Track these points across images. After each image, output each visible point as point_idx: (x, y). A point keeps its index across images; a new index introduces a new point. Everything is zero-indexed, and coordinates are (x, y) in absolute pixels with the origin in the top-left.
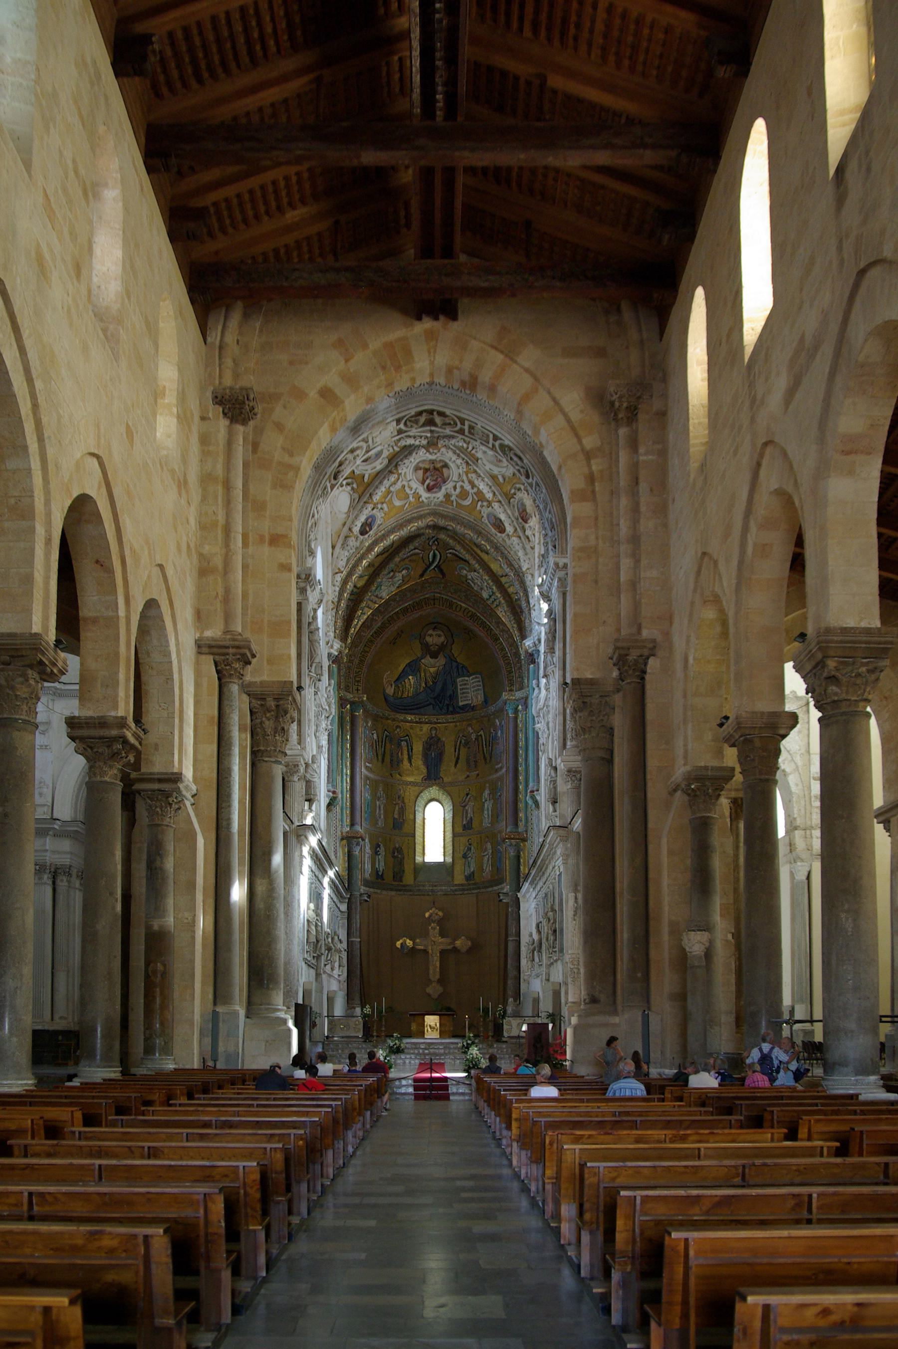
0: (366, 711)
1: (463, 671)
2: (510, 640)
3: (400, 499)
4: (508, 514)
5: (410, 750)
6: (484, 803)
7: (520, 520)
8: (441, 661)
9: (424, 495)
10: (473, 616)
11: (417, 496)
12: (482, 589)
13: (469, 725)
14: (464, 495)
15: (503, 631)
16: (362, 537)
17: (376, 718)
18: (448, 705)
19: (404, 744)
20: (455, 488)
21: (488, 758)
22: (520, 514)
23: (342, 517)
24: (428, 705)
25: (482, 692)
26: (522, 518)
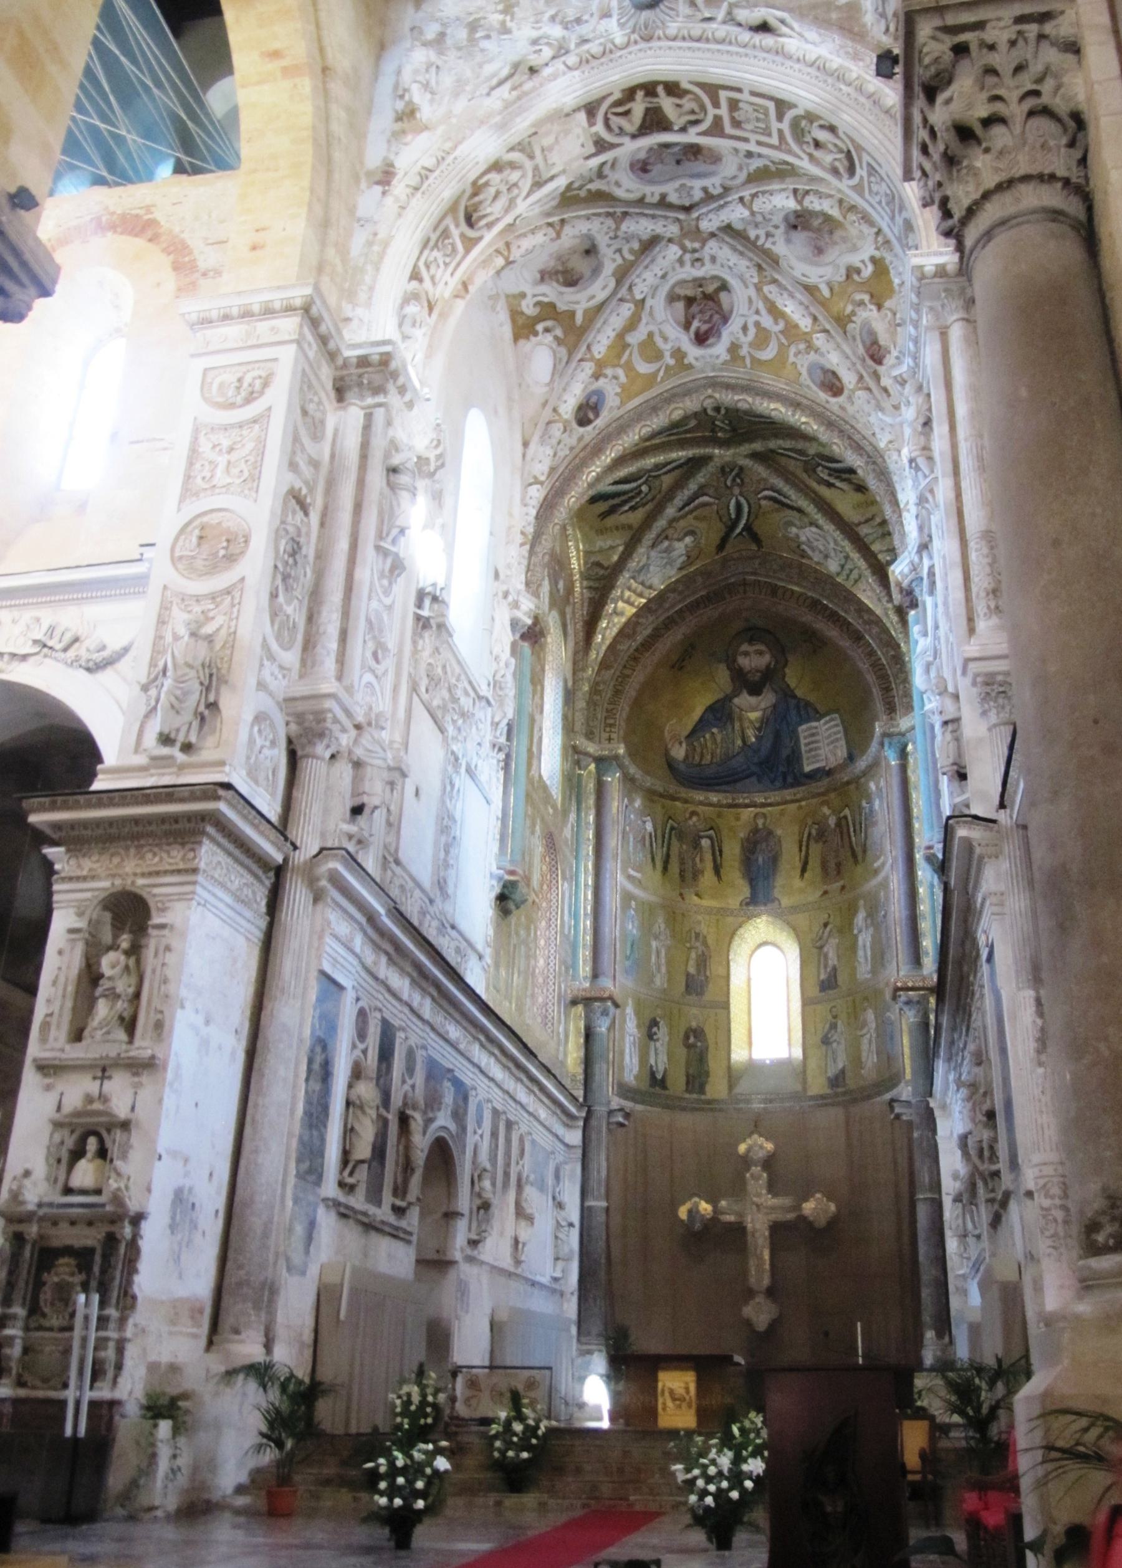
0: (628, 780)
1: (810, 712)
2: (884, 636)
3: (649, 360)
4: (843, 352)
5: (717, 852)
6: (856, 937)
7: (870, 362)
8: (768, 699)
9: (693, 352)
10: (815, 605)
11: (679, 354)
12: (826, 557)
13: (823, 803)
14: (763, 337)
15: (869, 623)
16: (582, 430)
17: (651, 796)
19: (705, 843)
20: (745, 328)
21: (860, 858)
22: (867, 350)
23: (540, 391)
24: (748, 777)
25: (843, 742)
26: (872, 357)
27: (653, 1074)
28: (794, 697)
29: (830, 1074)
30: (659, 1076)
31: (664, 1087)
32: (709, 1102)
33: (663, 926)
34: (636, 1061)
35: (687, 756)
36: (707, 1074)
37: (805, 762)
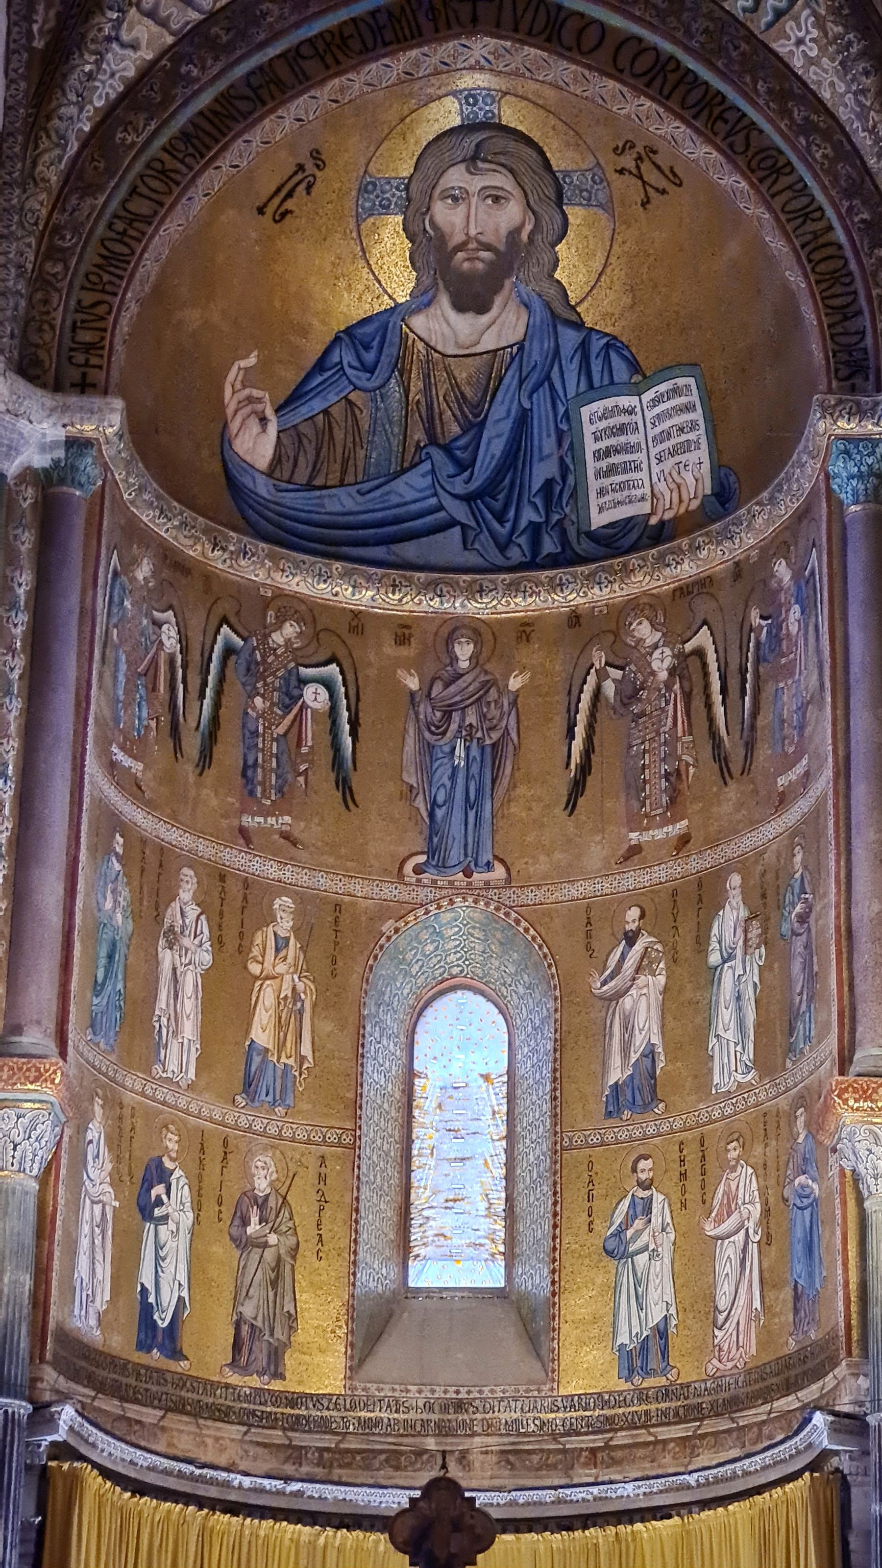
2: (843, 169)
18: (535, 530)
25: (702, 454)
27: (146, 1310)
28: (579, 325)
29: (623, 1338)
30: (163, 1320)
31: (177, 1354)
32: (293, 1400)
33: (192, 911)
34: (104, 1272)
35: (277, 460)
36: (292, 1319)
37: (594, 502)
